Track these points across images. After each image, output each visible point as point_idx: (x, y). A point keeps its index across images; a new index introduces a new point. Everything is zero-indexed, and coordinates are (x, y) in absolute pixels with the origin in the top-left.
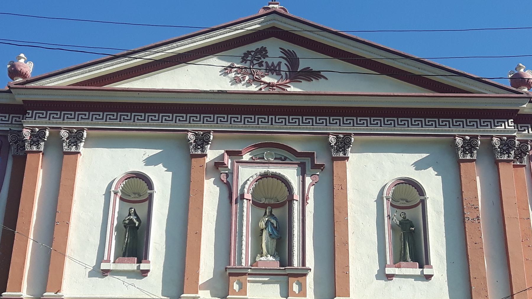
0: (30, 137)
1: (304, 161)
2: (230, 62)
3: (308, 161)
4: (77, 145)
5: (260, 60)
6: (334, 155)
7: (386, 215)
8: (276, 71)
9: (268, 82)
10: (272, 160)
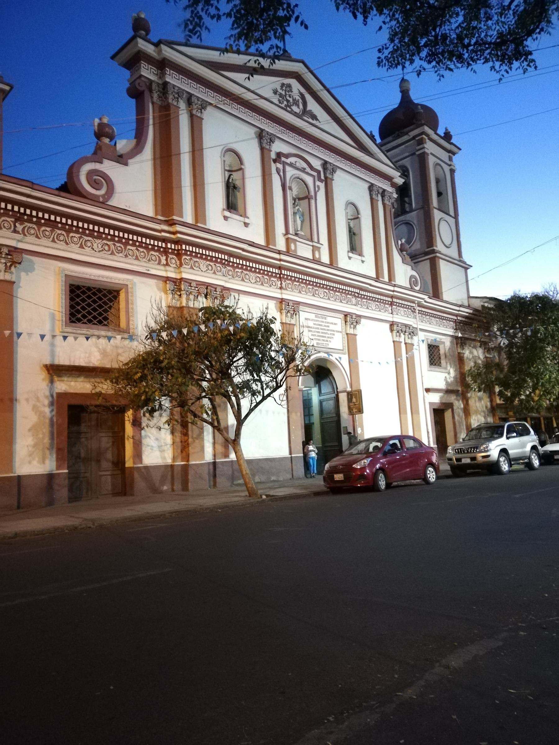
4: (201, 112)
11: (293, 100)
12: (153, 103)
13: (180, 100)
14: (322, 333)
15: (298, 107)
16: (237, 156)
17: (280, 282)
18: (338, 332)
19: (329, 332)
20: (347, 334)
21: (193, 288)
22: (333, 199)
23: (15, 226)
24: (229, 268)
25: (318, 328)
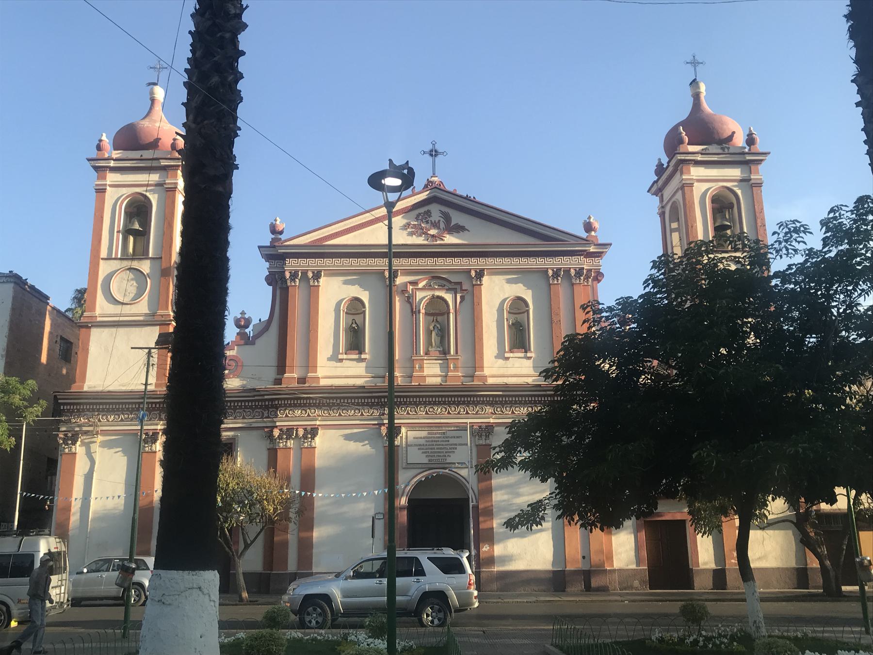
0: (289, 277)
1: (456, 287)
2: (408, 219)
3: (458, 287)
4: (318, 281)
5: (427, 219)
6: (474, 283)
7: (505, 318)
8: (437, 227)
9: (432, 234)
10: (437, 287)
11: (432, 223)
12: (280, 288)
14: (438, 449)
15: (439, 228)
17: (383, 409)
19: (448, 447)
20: (477, 445)
22: (480, 303)
23: (160, 415)
25: (433, 445)
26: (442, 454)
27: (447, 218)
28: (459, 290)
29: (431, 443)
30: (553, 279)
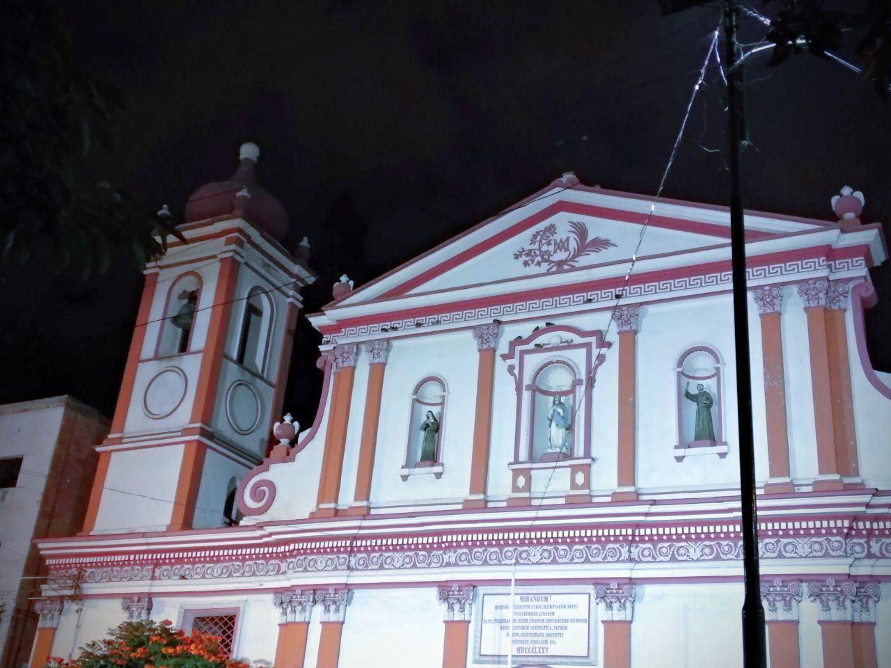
5: (549, 239)
12: (334, 373)
13: (351, 357)
15: (567, 249)
16: (423, 384)
18: (578, 621)
19: (552, 625)
20: (603, 622)
21: (299, 597)
23: (154, 572)
24: (360, 555)
25: (527, 620)
26: (541, 639)
27: (581, 231)
28: (594, 346)
29: (524, 617)
30: (764, 305)
